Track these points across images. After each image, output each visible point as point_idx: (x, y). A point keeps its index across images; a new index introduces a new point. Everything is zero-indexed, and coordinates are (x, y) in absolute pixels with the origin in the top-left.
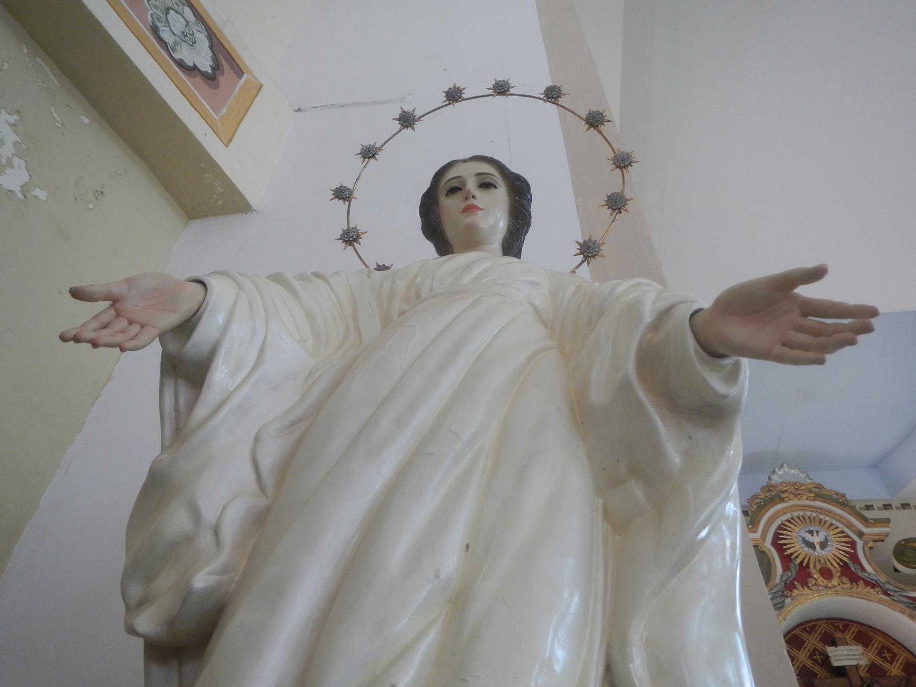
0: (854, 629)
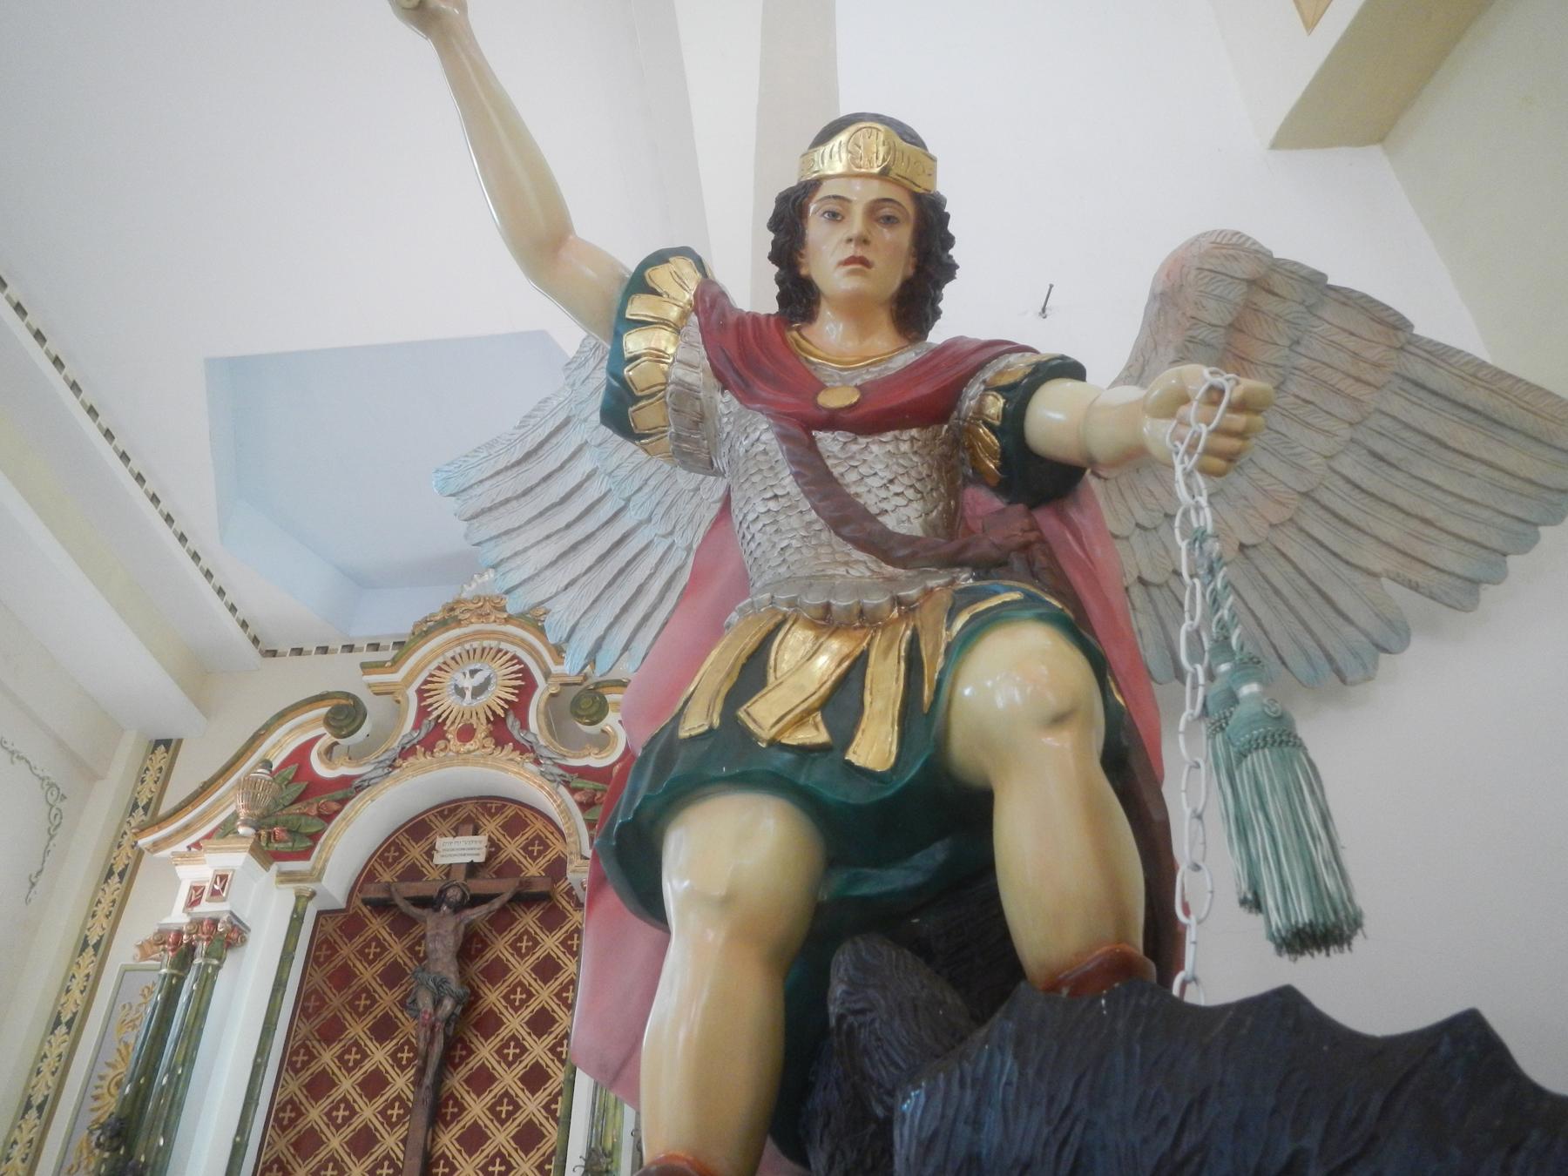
0: (510, 811)
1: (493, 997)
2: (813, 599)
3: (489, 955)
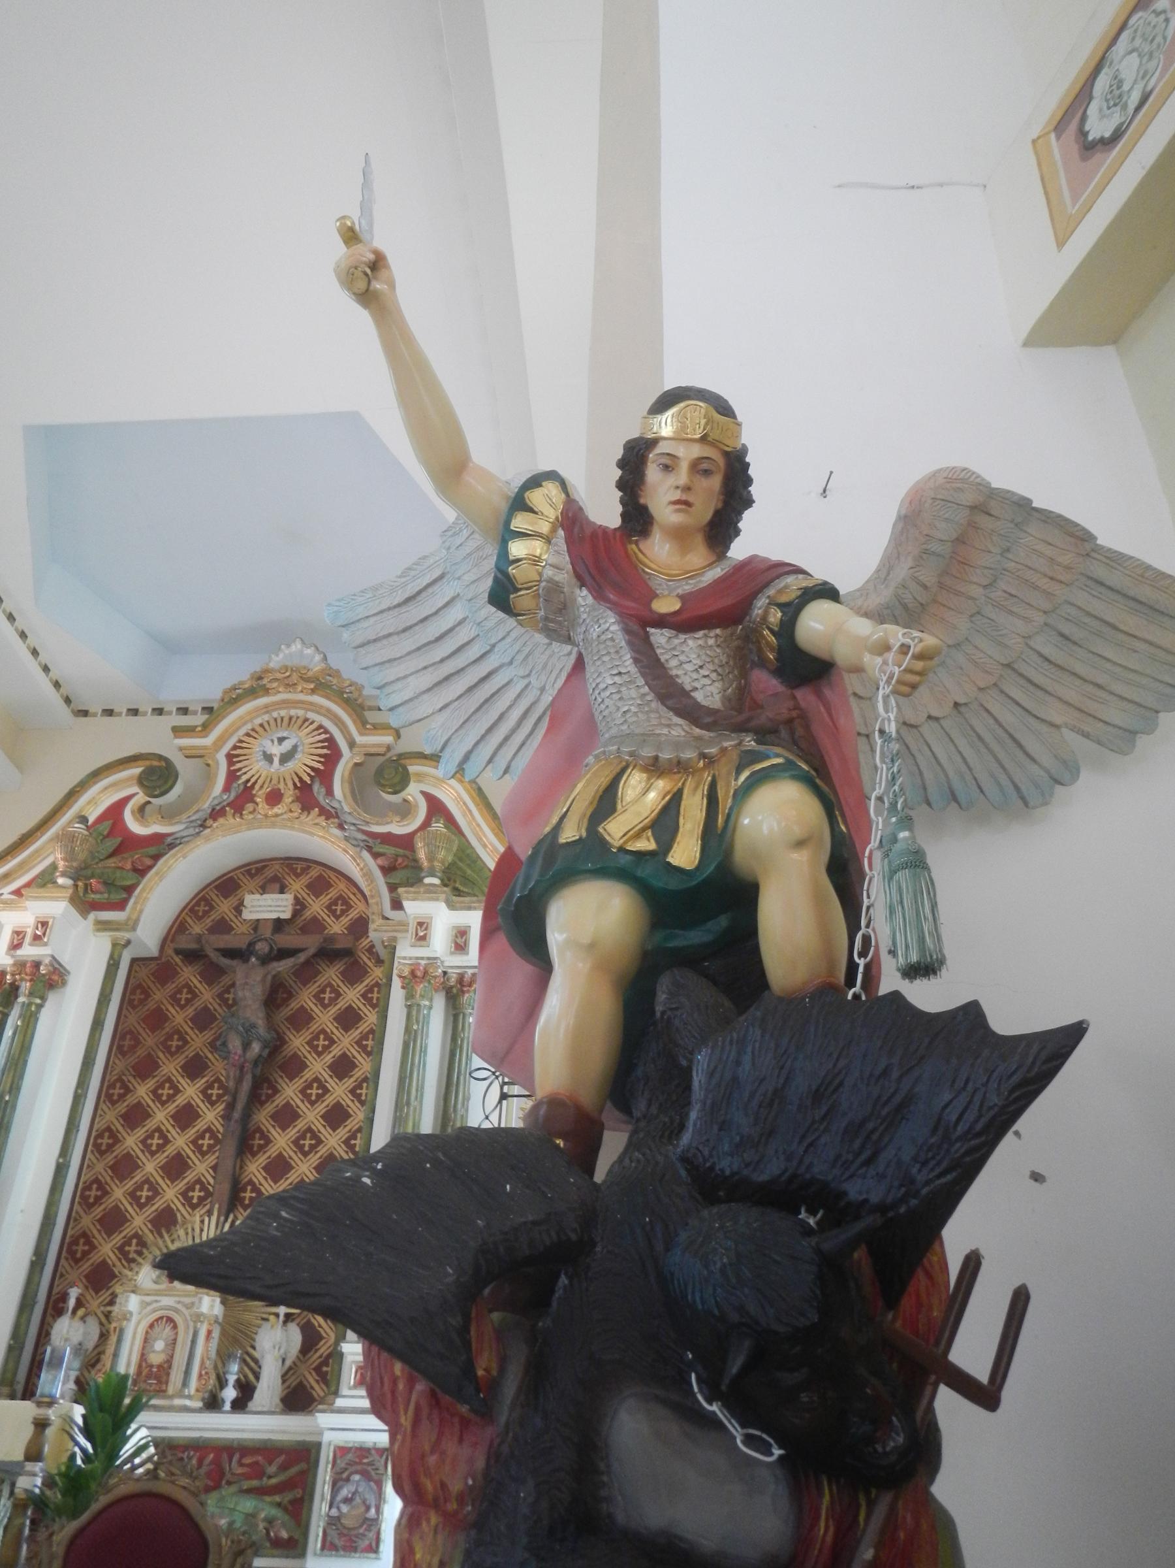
0: (314, 872)
1: (298, 1042)
2: (647, 752)
3: (294, 1005)
